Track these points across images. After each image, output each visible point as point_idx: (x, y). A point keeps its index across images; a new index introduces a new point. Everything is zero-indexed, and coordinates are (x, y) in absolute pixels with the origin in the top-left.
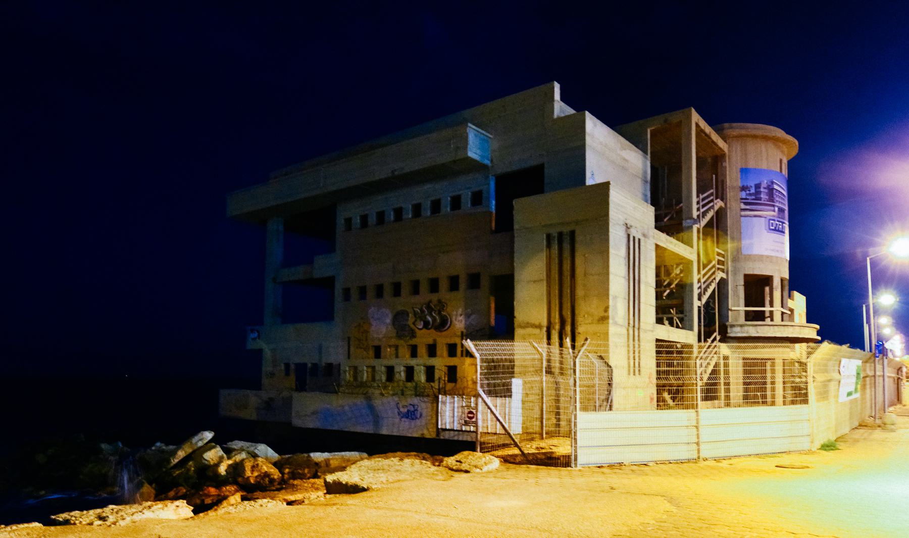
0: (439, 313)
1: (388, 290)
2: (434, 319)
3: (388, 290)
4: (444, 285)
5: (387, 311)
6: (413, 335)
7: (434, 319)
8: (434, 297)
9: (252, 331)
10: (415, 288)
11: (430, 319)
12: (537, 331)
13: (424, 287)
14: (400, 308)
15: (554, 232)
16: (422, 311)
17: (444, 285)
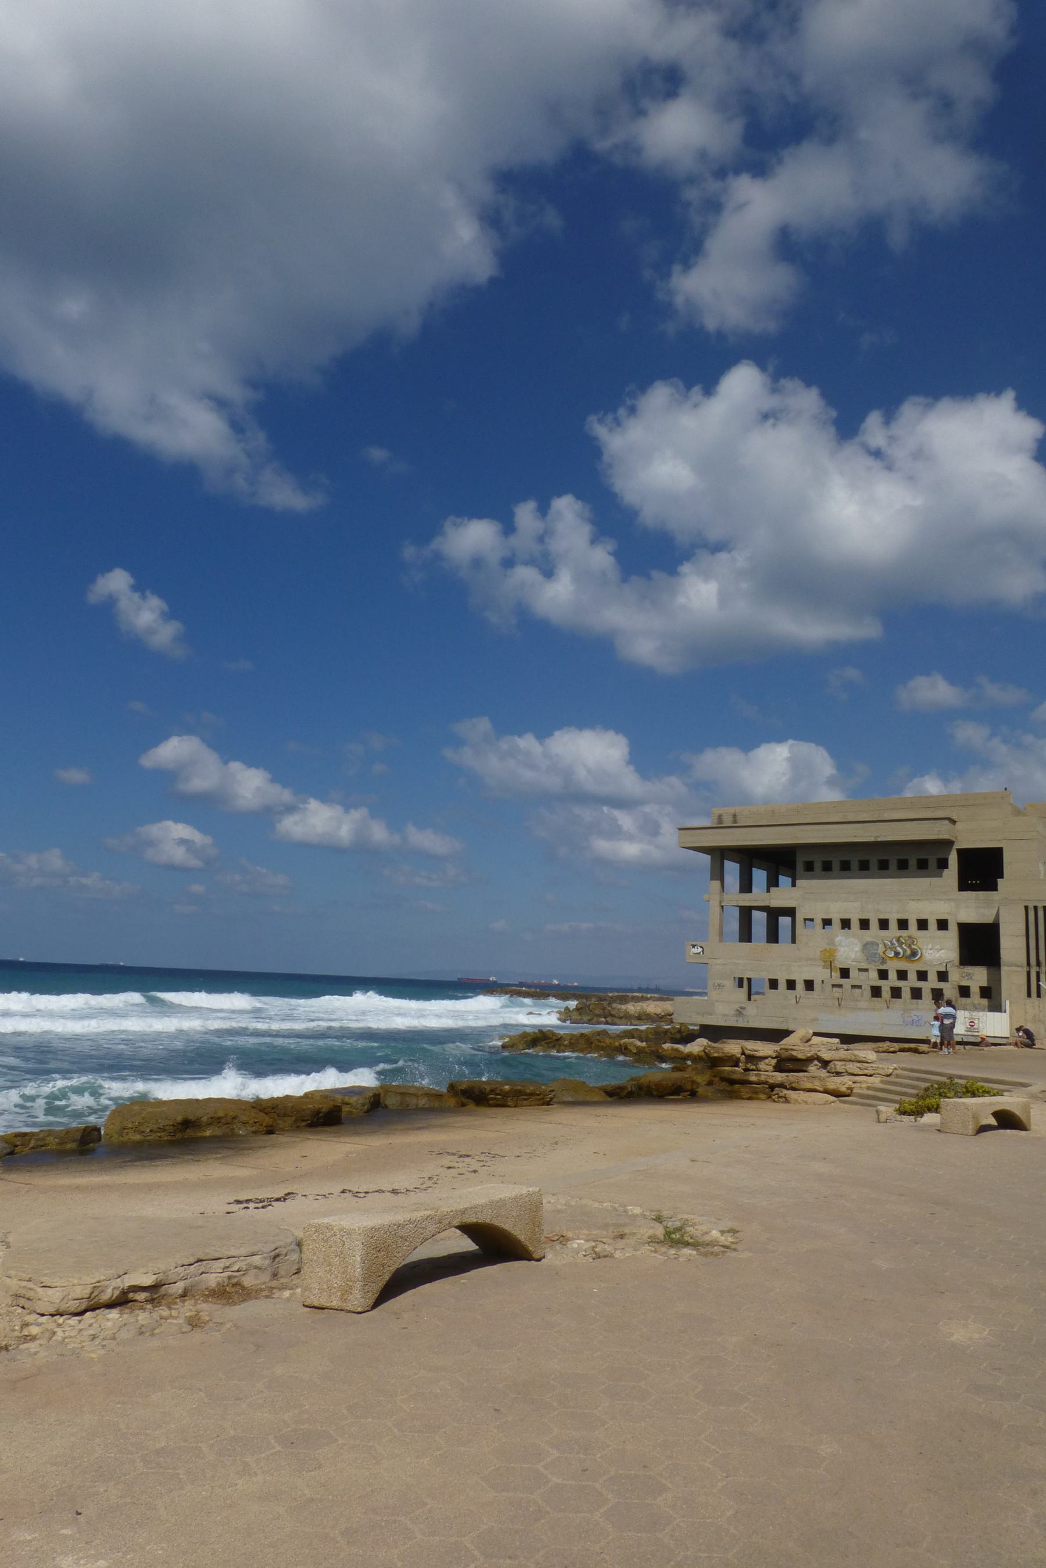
0: (910, 946)
1: (855, 924)
2: (905, 951)
3: (855, 924)
4: (913, 925)
5: (856, 941)
6: (884, 962)
7: (905, 951)
8: (904, 933)
9: (694, 946)
10: (884, 924)
11: (899, 949)
12: (1019, 969)
13: (893, 925)
14: (870, 939)
15: (1031, 906)
16: (892, 944)
17: (913, 925)
